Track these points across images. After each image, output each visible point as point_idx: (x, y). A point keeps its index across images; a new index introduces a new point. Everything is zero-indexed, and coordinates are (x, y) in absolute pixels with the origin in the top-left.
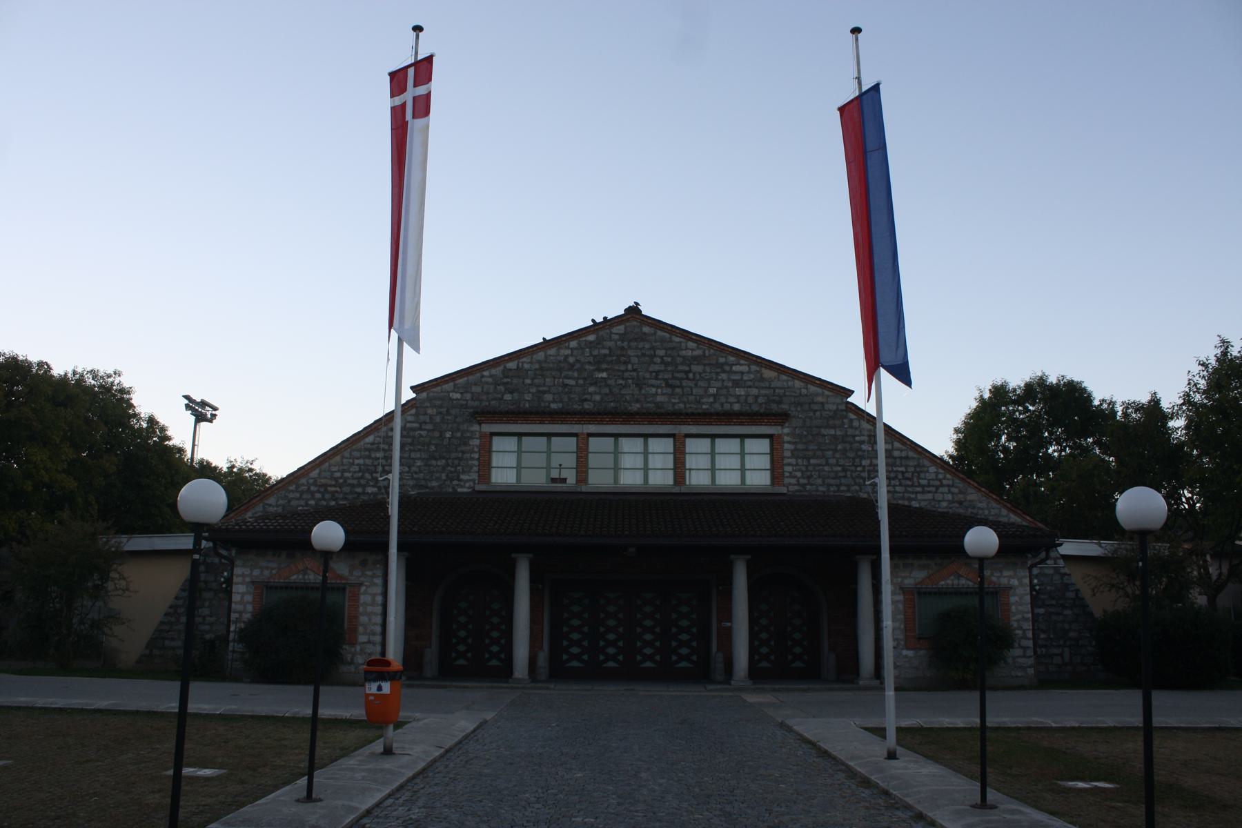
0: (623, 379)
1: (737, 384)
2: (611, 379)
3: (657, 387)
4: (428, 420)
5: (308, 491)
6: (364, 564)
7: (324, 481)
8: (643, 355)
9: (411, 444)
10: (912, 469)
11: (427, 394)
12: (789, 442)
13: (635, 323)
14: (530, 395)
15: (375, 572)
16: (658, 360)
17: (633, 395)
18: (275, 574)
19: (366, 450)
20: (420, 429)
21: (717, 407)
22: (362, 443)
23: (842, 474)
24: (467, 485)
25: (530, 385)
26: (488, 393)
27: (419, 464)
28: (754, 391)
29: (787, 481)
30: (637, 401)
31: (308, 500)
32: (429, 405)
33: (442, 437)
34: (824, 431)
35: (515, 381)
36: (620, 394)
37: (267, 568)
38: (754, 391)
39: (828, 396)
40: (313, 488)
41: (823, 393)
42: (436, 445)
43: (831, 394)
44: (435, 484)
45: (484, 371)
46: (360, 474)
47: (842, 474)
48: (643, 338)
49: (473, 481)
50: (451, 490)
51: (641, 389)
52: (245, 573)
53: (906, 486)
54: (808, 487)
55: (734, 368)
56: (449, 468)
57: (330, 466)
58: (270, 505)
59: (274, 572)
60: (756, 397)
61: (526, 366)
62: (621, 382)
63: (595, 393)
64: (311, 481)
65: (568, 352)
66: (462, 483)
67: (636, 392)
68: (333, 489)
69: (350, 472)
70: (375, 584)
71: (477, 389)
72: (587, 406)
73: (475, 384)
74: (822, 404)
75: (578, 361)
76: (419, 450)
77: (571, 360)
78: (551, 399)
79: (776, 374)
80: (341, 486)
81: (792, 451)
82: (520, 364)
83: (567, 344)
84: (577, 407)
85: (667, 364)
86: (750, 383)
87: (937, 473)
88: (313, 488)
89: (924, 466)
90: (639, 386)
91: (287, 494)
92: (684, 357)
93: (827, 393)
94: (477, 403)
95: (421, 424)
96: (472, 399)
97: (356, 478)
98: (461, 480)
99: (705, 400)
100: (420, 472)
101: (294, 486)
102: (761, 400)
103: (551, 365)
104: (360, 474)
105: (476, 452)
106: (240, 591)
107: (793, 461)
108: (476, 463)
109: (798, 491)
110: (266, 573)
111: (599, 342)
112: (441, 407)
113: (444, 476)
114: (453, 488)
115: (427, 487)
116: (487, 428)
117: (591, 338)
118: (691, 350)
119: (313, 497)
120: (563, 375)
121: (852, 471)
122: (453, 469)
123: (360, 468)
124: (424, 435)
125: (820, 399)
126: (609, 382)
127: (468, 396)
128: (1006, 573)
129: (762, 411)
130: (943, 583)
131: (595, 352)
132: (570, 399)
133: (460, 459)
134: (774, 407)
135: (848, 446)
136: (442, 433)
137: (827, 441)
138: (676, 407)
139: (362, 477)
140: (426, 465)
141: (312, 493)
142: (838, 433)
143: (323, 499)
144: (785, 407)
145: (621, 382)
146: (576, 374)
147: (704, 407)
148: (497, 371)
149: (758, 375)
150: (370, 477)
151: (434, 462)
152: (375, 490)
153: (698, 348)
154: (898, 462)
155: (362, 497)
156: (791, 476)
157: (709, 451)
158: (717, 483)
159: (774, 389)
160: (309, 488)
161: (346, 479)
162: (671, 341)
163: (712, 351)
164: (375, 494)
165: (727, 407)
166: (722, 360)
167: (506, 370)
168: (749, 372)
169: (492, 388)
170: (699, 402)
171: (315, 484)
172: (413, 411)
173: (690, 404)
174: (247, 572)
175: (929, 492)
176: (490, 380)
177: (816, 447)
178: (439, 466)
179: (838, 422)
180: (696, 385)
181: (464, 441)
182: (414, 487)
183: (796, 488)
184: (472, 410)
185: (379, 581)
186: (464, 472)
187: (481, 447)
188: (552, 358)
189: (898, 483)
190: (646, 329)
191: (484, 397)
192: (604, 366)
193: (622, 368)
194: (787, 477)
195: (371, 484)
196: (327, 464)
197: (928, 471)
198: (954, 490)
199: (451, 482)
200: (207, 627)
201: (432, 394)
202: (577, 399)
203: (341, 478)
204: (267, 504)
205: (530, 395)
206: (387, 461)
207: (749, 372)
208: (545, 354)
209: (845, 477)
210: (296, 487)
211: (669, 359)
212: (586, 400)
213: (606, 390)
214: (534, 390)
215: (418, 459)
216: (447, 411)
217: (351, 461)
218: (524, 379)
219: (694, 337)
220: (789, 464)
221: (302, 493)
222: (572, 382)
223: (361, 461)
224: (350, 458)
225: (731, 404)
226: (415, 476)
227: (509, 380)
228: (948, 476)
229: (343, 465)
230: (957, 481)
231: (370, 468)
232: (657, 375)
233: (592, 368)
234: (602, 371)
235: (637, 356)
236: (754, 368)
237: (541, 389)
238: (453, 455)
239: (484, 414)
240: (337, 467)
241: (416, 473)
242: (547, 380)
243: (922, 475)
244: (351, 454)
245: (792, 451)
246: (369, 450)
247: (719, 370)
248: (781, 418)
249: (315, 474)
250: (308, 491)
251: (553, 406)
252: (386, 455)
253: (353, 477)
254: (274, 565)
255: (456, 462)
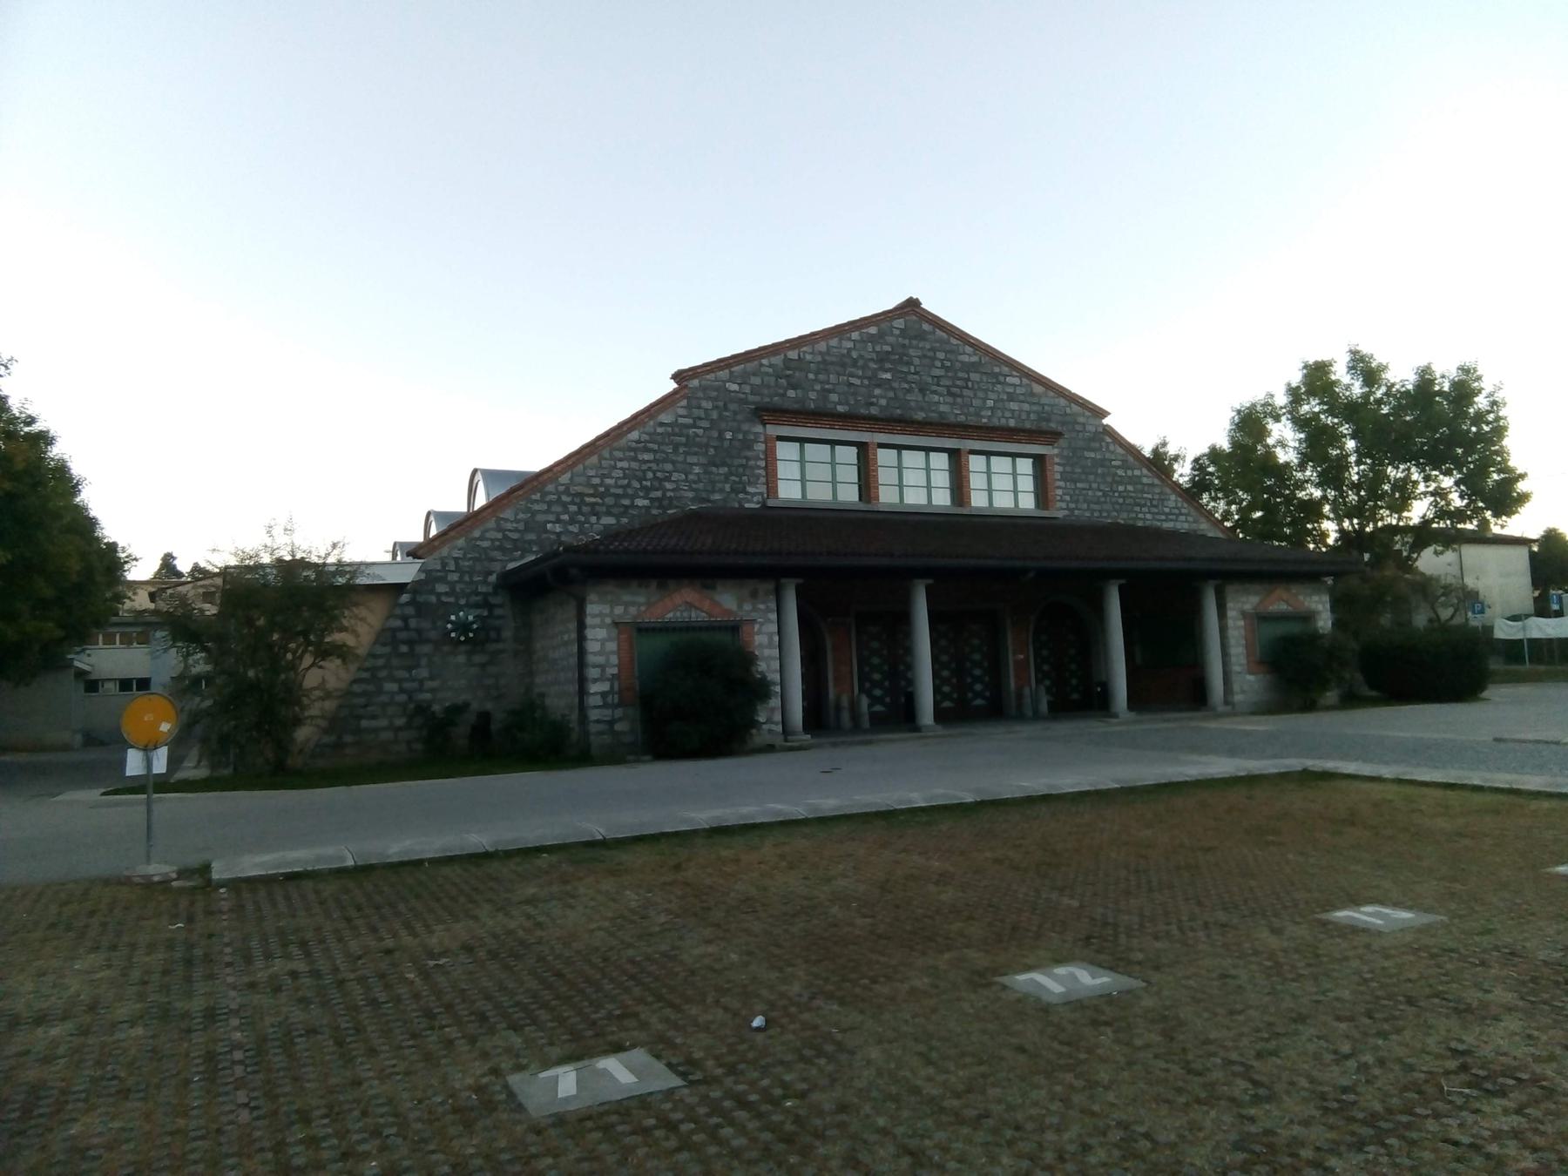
0: (908, 382)
1: (1011, 397)
2: (895, 381)
3: (940, 395)
4: (703, 416)
5: (559, 501)
6: (754, 595)
7: (579, 489)
8: (925, 356)
9: (685, 445)
10: (1156, 497)
11: (700, 382)
12: (1058, 464)
13: (914, 318)
14: (815, 393)
15: (769, 604)
16: (938, 364)
17: (917, 401)
18: (645, 612)
19: (631, 449)
20: (694, 426)
21: (995, 422)
22: (623, 442)
23: (1103, 499)
24: (755, 499)
25: (813, 380)
26: (769, 387)
27: (697, 471)
28: (1026, 407)
29: (1059, 504)
30: (922, 409)
31: (558, 514)
32: (702, 396)
33: (721, 437)
34: (1087, 454)
35: (797, 374)
36: (906, 400)
37: (633, 604)
38: (1026, 407)
39: (1088, 417)
40: (565, 498)
41: (1084, 413)
42: (715, 448)
43: (1090, 414)
44: (717, 497)
45: (763, 358)
46: (626, 482)
47: (1103, 499)
48: (922, 336)
49: (762, 494)
50: (737, 505)
51: (924, 395)
52: (604, 611)
53: (1153, 513)
54: (1076, 512)
55: (1008, 379)
56: (733, 478)
57: (585, 468)
58: (506, 520)
59: (643, 608)
60: (1028, 413)
61: (808, 357)
62: (906, 386)
63: (882, 397)
64: (561, 488)
65: (850, 345)
66: (749, 497)
67: (920, 399)
68: (592, 500)
69: (612, 478)
70: (770, 621)
71: (756, 381)
72: (874, 411)
73: (754, 374)
74: (1084, 424)
75: (861, 357)
76: (696, 454)
77: (854, 354)
78: (837, 400)
79: (1044, 389)
80: (602, 496)
81: (1061, 473)
82: (801, 354)
83: (848, 335)
84: (863, 411)
85: (947, 369)
86: (1022, 398)
87: (1176, 501)
88: (565, 498)
89: (1166, 494)
90: (922, 391)
91: (529, 505)
92: (962, 362)
93: (1087, 413)
94: (757, 398)
95: (694, 419)
96: (752, 393)
97: (621, 487)
98: (747, 493)
99: (983, 413)
100: (700, 481)
101: (539, 495)
102: (1033, 416)
103: (834, 359)
104: (626, 482)
105: (762, 460)
106: (599, 637)
107: (1062, 484)
108: (762, 472)
109: (1068, 516)
110: (633, 610)
111: (881, 335)
112: (715, 399)
113: (727, 487)
114: (739, 503)
115: (709, 501)
116: (773, 430)
117: (873, 330)
118: (968, 357)
119: (566, 511)
120: (847, 372)
121: (1110, 496)
122: (737, 479)
123: (624, 474)
124: (701, 434)
125: (1081, 420)
126: (896, 385)
127: (747, 389)
128: (1316, 598)
129: (1034, 428)
130: (1271, 608)
131: (878, 348)
132: (856, 401)
133: (744, 466)
134: (1044, 425)
135: (1106, 470)
136: (721, 433)
137: (1089, 464)
138: (959, 420)
139: (629, 485)
140: (706, 472)
141: (565, 505)
142: (1098, 457)
143: (580, 512)
144: (1053, 425)
145: (906, 386)
146: (860, 373)
147: (984, 420)
148: (777, 360)
149: (1029, 390)
150: (639, 487)
151: (714, 469)
152: (646, 502)
153: (975, 354)
154: (1146, 489)
155: (630, 511)
156: (1061, 501)
157: (1011, 472)
158: (995, 506)
159: (1043, 405)
160: (560, 498)
161: (608, 488)
162: (948, 342)
163: (987, 358)
164: (648, 508)
165: (1003, 421)
166: (997, 370)
167: (787, 360)
168: (1020, 385)
169: (772, 380)
170: (978, 415)
171: (567, 492)
172: (684, 403)
173: (971, 416)
174: (606, 609)
175: (1171, 520)
176: (771, 370)
177: (1079, 470)
178: (721, 474)
179: (1097, 445)
180: (975, 395)
181: (748, 444)
182: (693, 500)
183: (1066, 512)
184: (753, 407)
185: (774, 616)
186: (750, 483)
187: (766, 452)
188: (835, 350)
189: (1147, 511)
190: (926, 327)
191: (766, 391)
192: (888, 365)
193: (905, 369)
194: (1059, 501)
195: (641, 494)
196: (581, 467)
197: (1169, 499)
198: (1190, 519)
199: (737, 495)
200: (428, 696)
201: (704, 382)
202: (862, 402)
203: (601, 485)
204: (503, 519)
205: (815, 393)
206: (658, 465)
207: (1020, 385)
208: (827, 345)
209: (1105, 502)
210: (541, 496)
211: (949, 364)
212: (872, 404)
213: (891, 394)
214: (818, 387)
215: (695, 464)
216: (725, 405)
217: (613, 463)
218: (807, 373)
219: (972, 341)
220: (1059, 487)
221: (550, 504)
222: (857, 382)
223: (625, 464)
224: (611, 460)
225: (1007, 418)
226: (694, 486)
227: (791, 372)
228: (1185, 505)
229: (601, 467)
230: (1192, 510)
231: (637, 473)
232: (938, 382)
233: (875, 366)
234: (886, 371)
235: (918, 357)
236: (1025, 381)
237: (827, 386)
238: (737, 462)
239: (768, 413)
240: (594, 471)
241: (695, 482)
242: (831, 376)
243: (1165, 503)
244: (611, 453)
245: (1061, 473)
246: (634, 450)
247: (994, 381)
248: (1051, 437)
249: (565, 479)
250: (559, 501)
251: (840, 409)
252: (657, 457)
253: (617, 486)
254: (641, 599)
255: (741, 470)
